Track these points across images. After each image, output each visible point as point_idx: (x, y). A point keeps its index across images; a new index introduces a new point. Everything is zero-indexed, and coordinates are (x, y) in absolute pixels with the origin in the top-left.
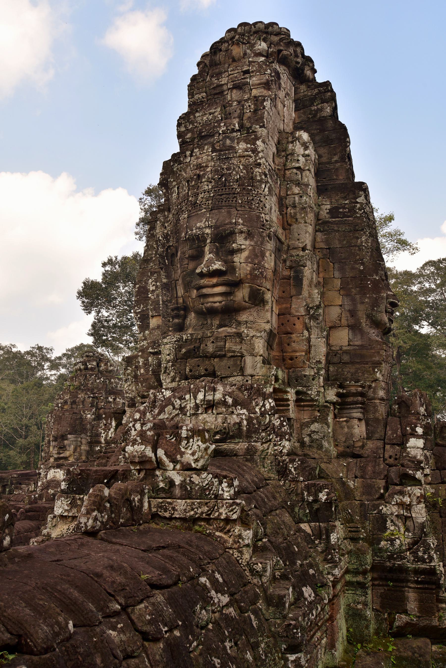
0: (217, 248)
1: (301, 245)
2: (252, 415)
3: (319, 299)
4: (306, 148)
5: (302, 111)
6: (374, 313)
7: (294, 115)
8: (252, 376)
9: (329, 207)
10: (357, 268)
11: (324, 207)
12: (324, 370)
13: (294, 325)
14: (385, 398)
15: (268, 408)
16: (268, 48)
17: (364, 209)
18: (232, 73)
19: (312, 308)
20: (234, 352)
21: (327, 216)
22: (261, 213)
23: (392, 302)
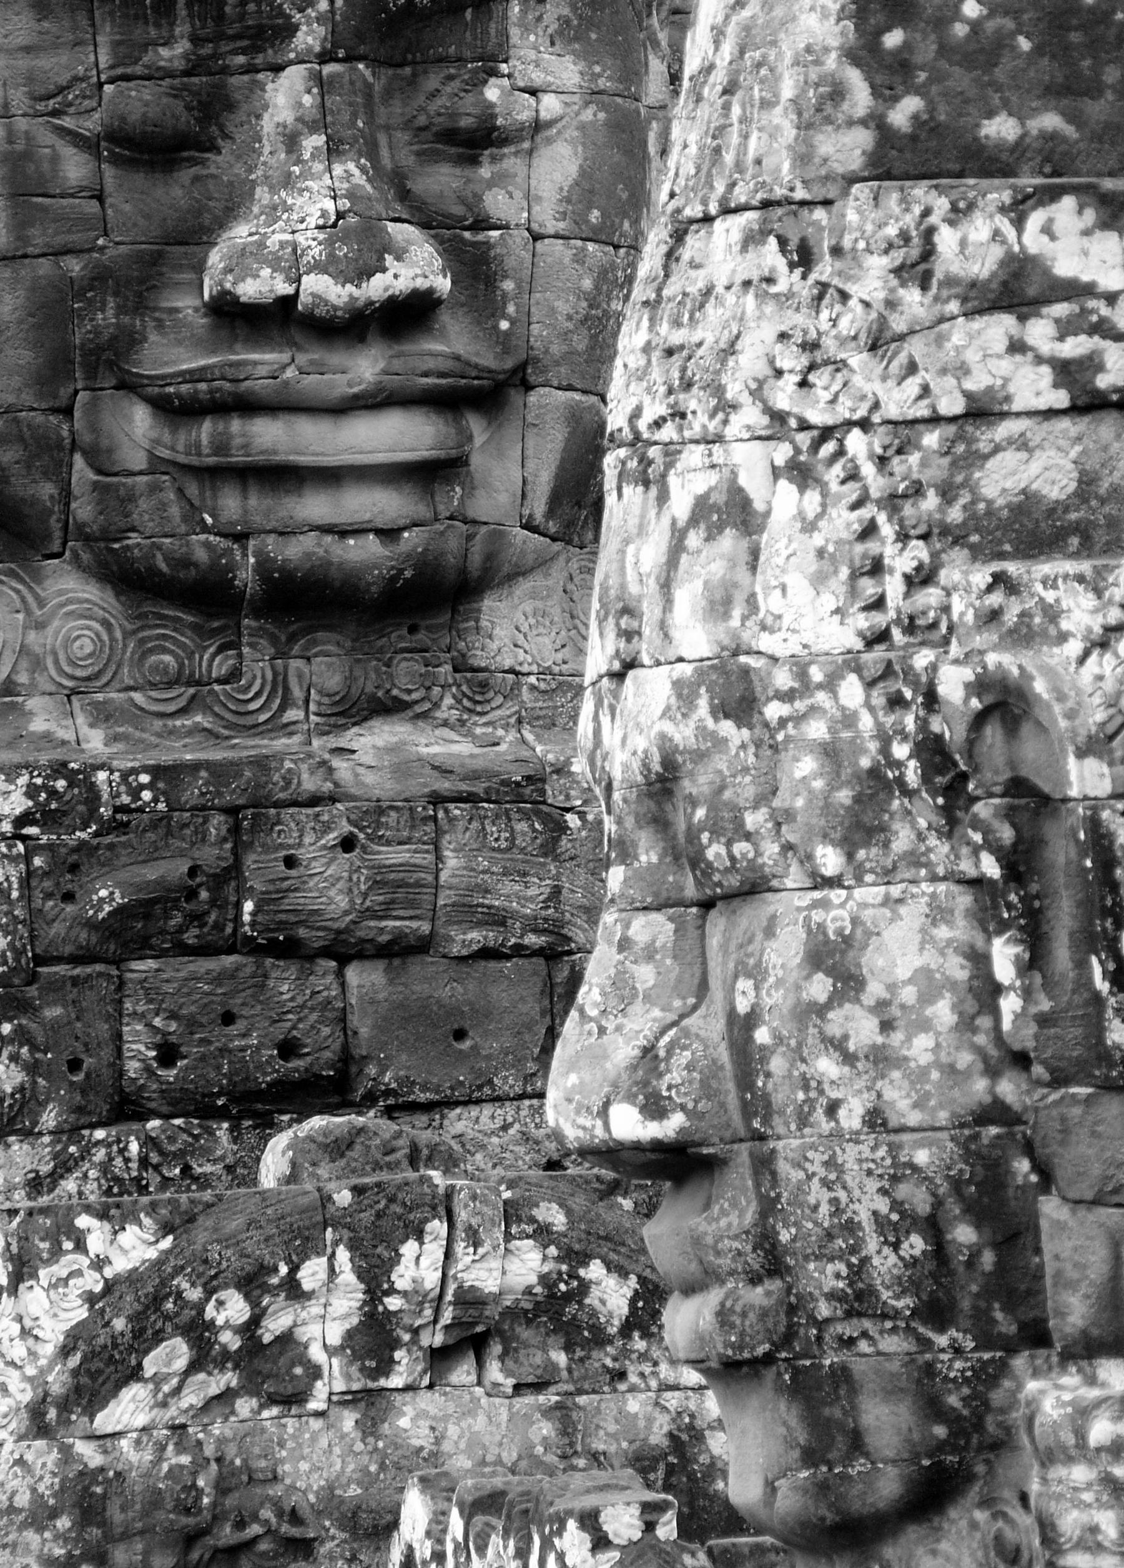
20: (498, 919)
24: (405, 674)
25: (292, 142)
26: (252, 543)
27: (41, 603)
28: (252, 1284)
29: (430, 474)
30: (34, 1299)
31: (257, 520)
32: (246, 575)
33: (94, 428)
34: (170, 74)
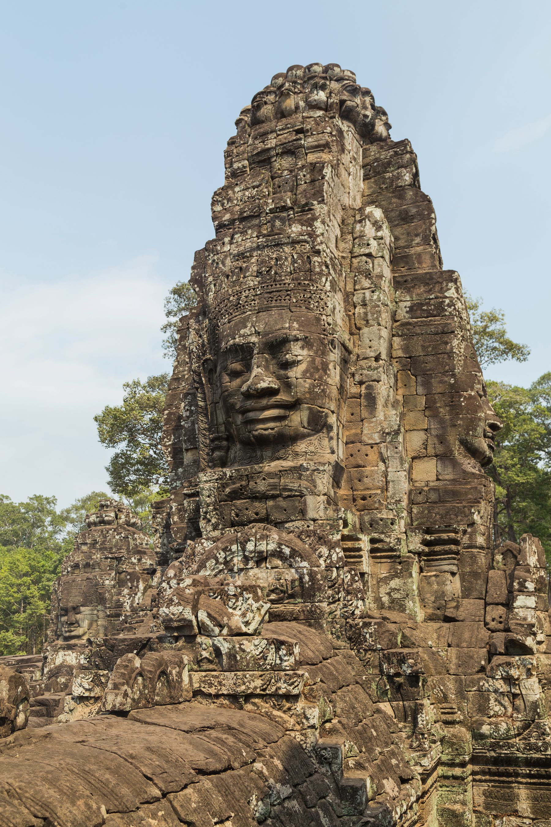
0: (267, 360)
1: (373, 354)
2: (315, 569)
3: (398, 422)
4: (379, 228)
5: (372, 180)
6: (469, 439)
7: (362, 185)
8: (314, 520)
9: (408, 304)
10: (446, 382)
11: (402, 304)
12: (405, 512)
13: (367, 455)
14: (485, 545)
15: (336, 559)
16: (327, 98)
17: (454, 305)
18: (281, 132)
19: (388, 434)
20: (291, 490)
21: (407, 316)
22: (322, 315)
23: (493, 424)
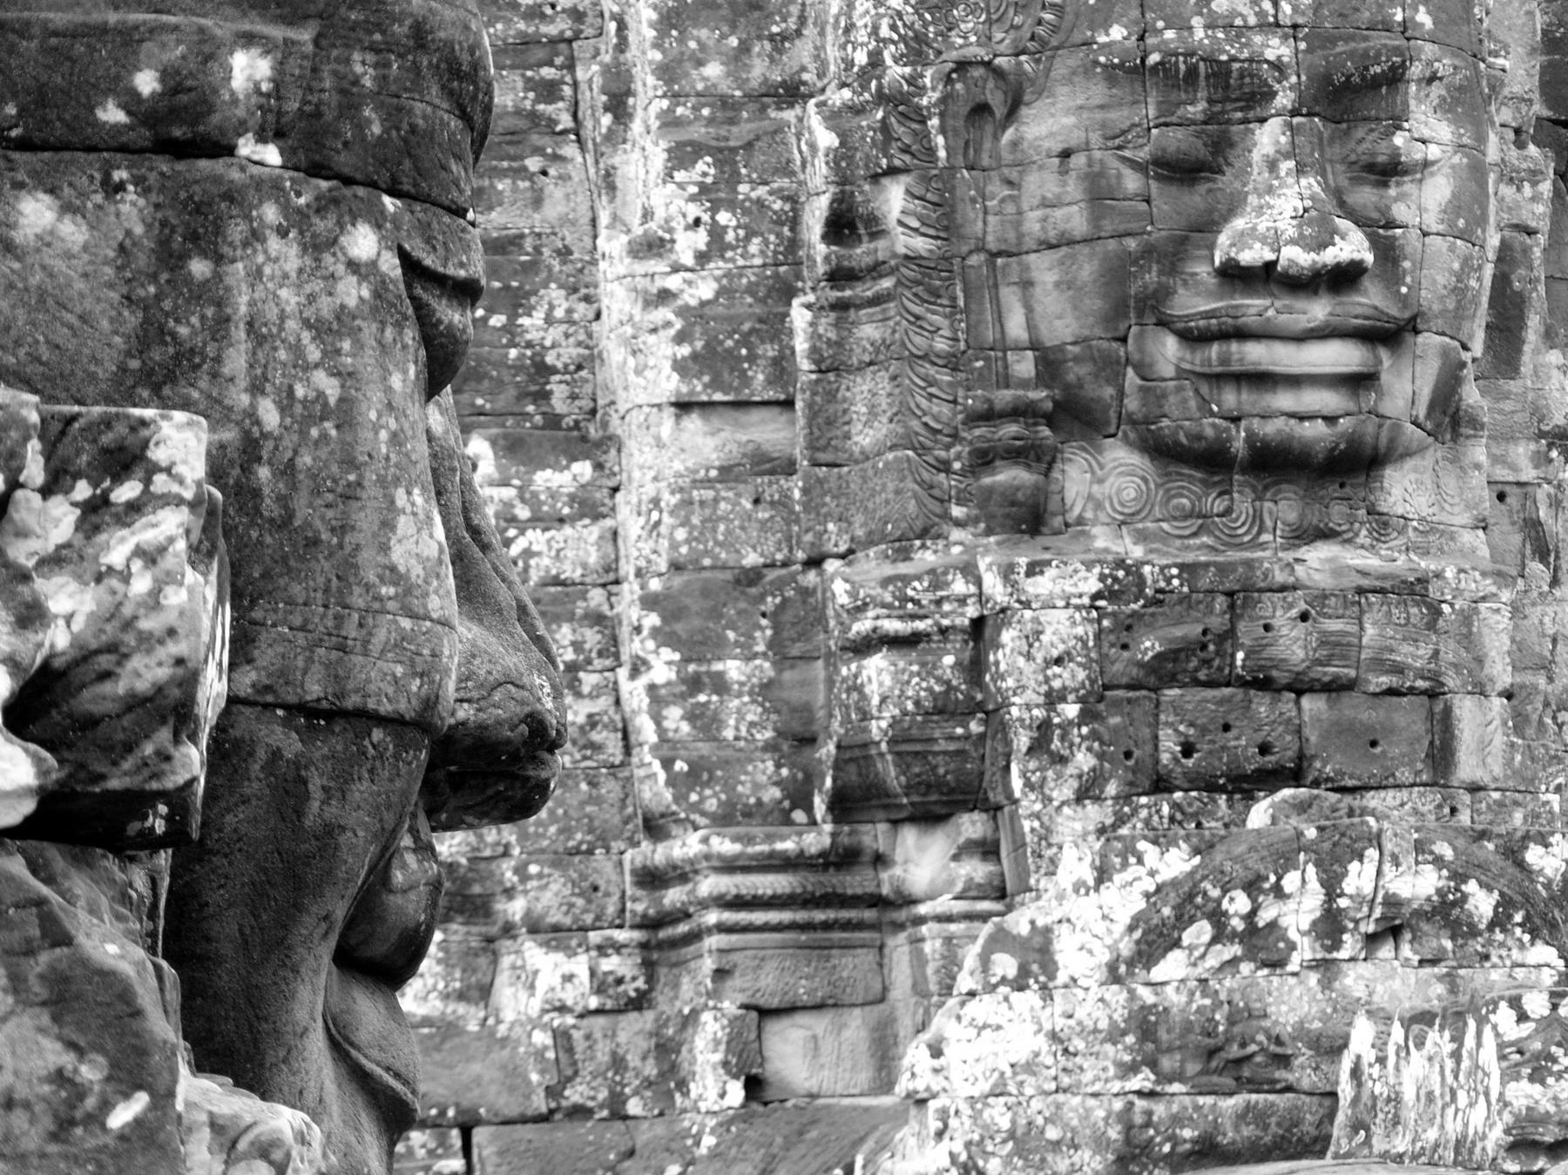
20: (1399, 669)
24: (1337, 514)
25: (1272, 165)
26: (1243, 423)
27: (1101, 467)
28: (1252, 887)
29: (1358, 382)
30: (1110, 893)
31: (1247, 408)
32: (1239, 445)
33: (1141, 350)
34: (1193, 123)
